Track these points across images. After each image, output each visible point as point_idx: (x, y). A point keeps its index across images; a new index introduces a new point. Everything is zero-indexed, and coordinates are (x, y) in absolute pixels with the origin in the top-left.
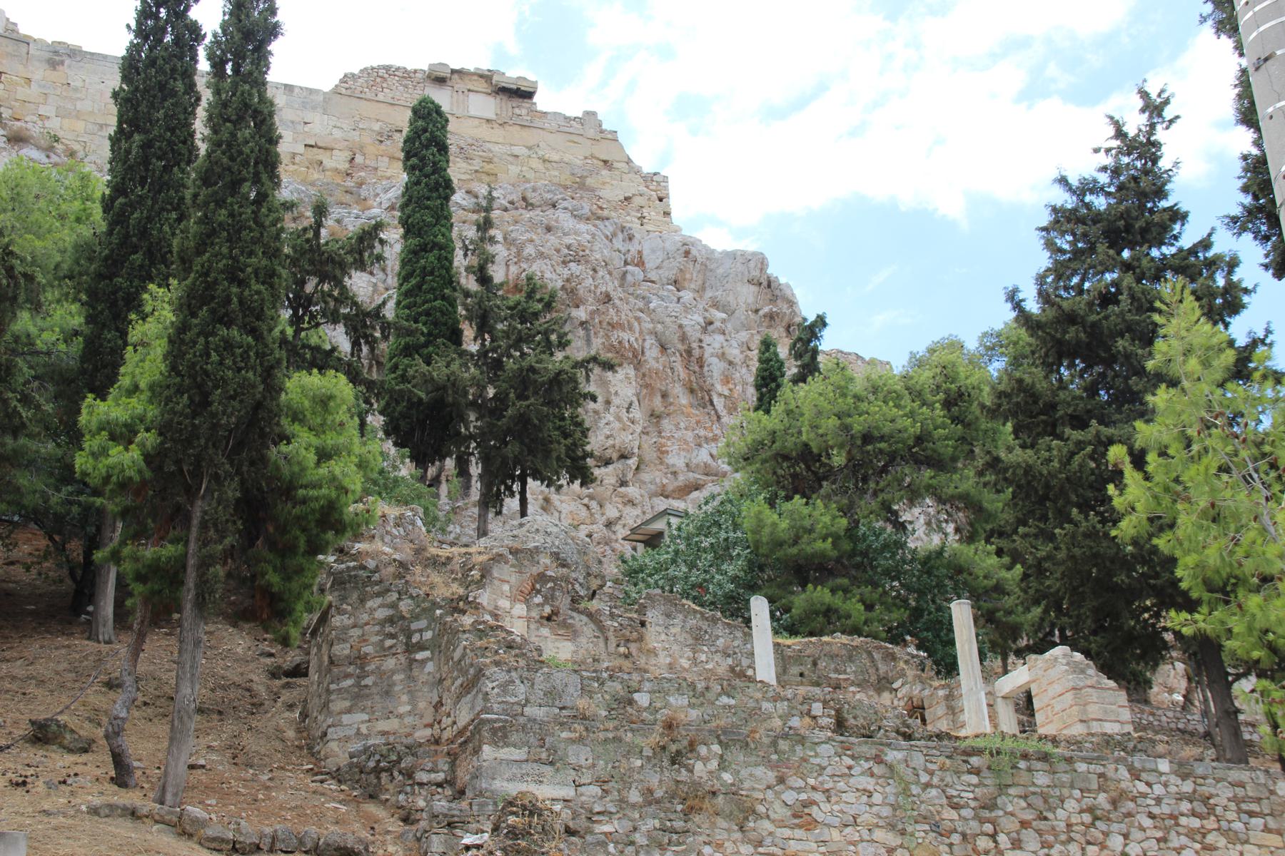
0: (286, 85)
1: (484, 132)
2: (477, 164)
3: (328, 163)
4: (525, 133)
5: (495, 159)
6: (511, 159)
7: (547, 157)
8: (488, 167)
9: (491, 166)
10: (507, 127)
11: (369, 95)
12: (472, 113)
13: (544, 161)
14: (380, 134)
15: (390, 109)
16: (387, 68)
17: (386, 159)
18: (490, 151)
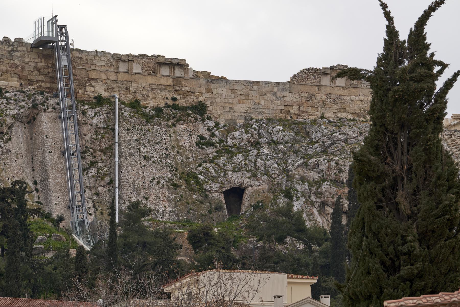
0: (277, 83)
1: (341, 92)
2: (340, 105)
3: (292, 112)
4: (355, 91)
5: (346, 103)
6: (350, 102)
7: (362, 99)
8: (343, 106)
9: (344, 105)
10: (349, 89)
11: (303, 83)
12: (337, 85)
13: (362, 101)
14: (307, 98)
15: (310, 87)
16: (308, 70)
17: (310, 108)
18: (343, 99)
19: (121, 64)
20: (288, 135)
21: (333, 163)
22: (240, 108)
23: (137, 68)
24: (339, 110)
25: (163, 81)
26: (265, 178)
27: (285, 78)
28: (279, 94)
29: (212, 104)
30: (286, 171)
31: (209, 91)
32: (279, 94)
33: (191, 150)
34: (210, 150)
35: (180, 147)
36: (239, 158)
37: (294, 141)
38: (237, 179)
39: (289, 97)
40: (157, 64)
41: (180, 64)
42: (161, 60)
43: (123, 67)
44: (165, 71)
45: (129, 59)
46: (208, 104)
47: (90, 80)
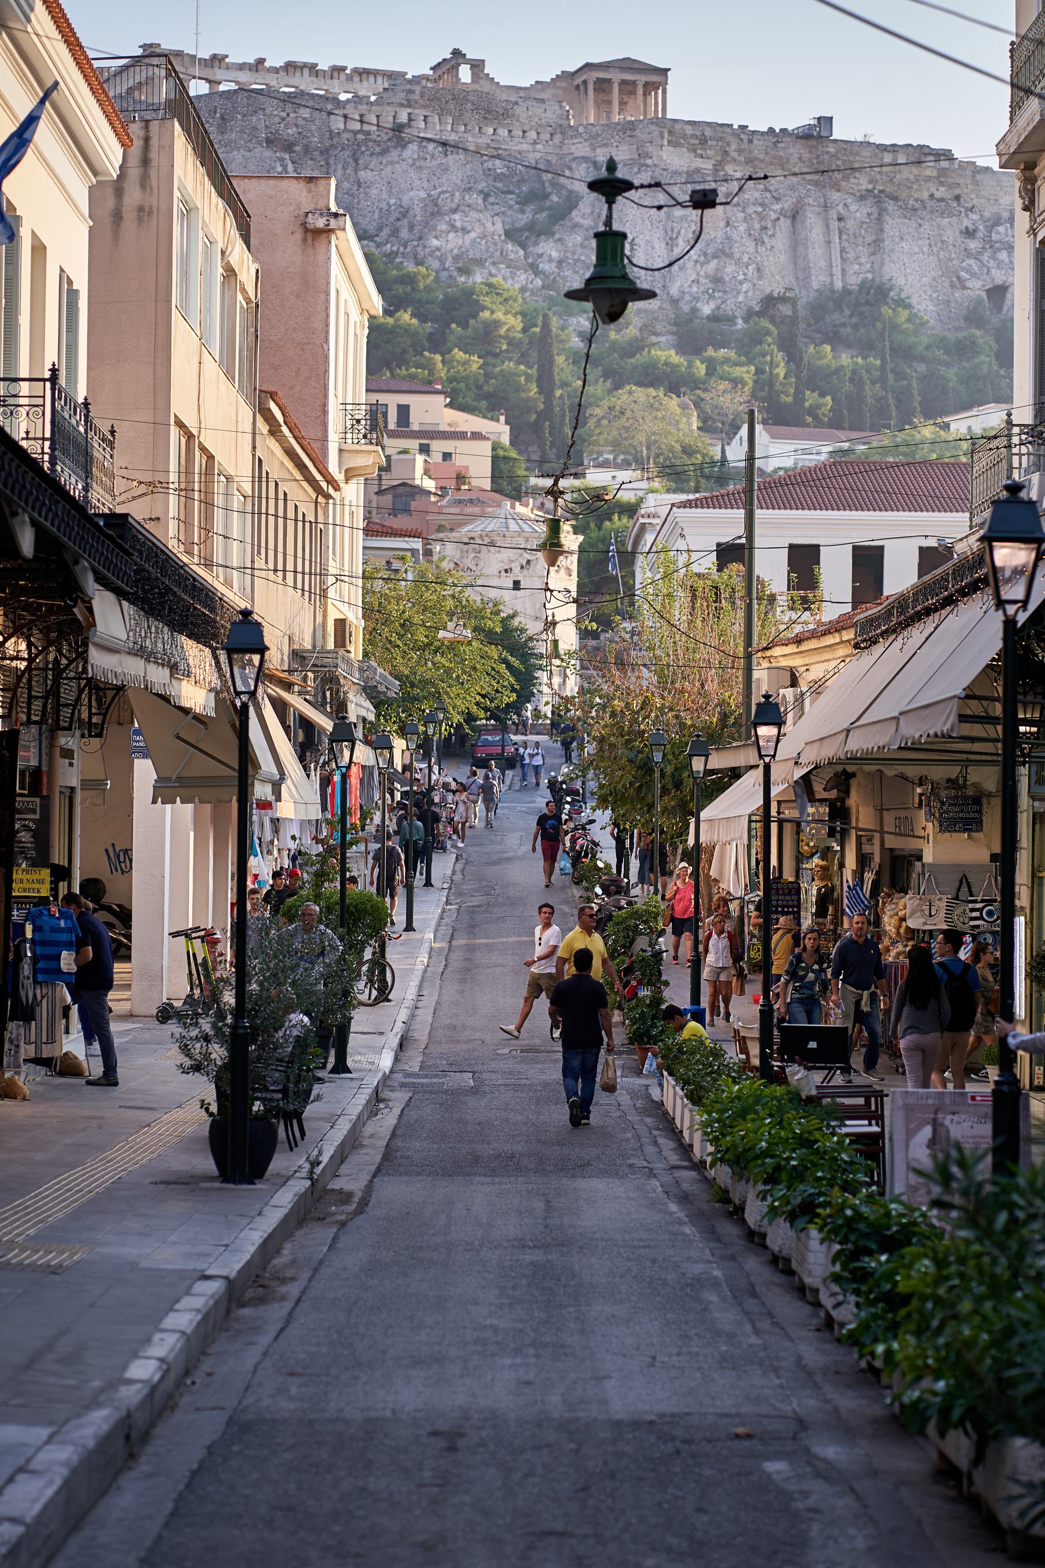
19: (886, 154)
25: (928, 172)
31: (976, 183)
34: (973, 245)
40: (921, 155)
42: (927, 151)
46: (973, 196)
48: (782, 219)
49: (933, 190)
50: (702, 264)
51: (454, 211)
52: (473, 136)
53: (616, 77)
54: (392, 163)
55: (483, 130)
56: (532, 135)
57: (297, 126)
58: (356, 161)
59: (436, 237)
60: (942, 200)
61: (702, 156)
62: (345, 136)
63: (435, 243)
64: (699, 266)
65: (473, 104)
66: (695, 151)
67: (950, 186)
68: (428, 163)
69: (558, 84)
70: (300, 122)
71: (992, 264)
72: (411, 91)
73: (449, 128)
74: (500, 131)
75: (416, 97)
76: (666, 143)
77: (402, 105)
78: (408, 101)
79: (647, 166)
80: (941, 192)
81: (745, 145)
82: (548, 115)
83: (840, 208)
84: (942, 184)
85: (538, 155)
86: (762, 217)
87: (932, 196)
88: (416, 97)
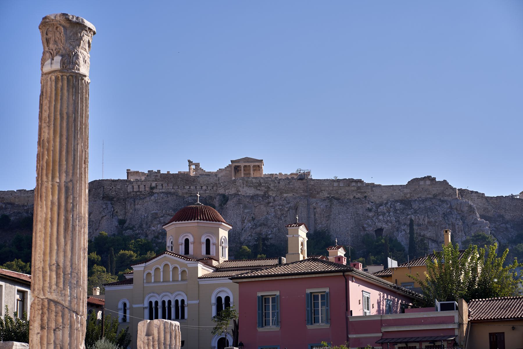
19: (335, 183)
20: (402, 206)
21: (417, 217)
22: (385, 197)
23: (341, 185)
24: (428, 194)
25: (353, 188)
26: (390, 224)
27: (405, 183)
28: (401, 190)
29: (373, 196)
30: (398, 221)
31: (372, 191)
32: (401, 190)
33: (363, 215)
34: (370, 214)
35: (357, 214)
36: (381, 217)
37: (404, 209)
38: (379, 225)
39: (406, 191)
41: (360, 181)
42: (351, 180)
43: (336, 184)
44: (354, 184)
45: (339, 181)
47: (322, 191)
48: (291, 210)
49: (355, 195)
50: (254, 229)
51: (162, 217)
52: (181, 190)
53: (242, 164)
54: (147, 202)
55: (185, 187)
56: (204, 188)
57: (116, 191)
58: (135, 202)
59: (154, 227)
60: (359, 198)
61: (259, 190)
62: (133, 193)
63: (153, 228)
64: (252, 230)
65: (181, 178)
66: (257, 188)
67: (361, 193)
68: (160, 201)
69: (227, 169)
70: (117, 190)
71: (377, 221)
72: (157, 176)
73: (171, 187)
74: (192, 187)
75: (159, 177)
76: (245, 186)
77: (153, 181)
78: (156, 179)
79: (239, 195)
80: (359, 195)
81: (277, 184)
82: (211, 180)
83: (314, 204)
84: (359, 192)
85: (207, 195)
86: (281, 210)
87: (354, 197)
88: (159, 177)
